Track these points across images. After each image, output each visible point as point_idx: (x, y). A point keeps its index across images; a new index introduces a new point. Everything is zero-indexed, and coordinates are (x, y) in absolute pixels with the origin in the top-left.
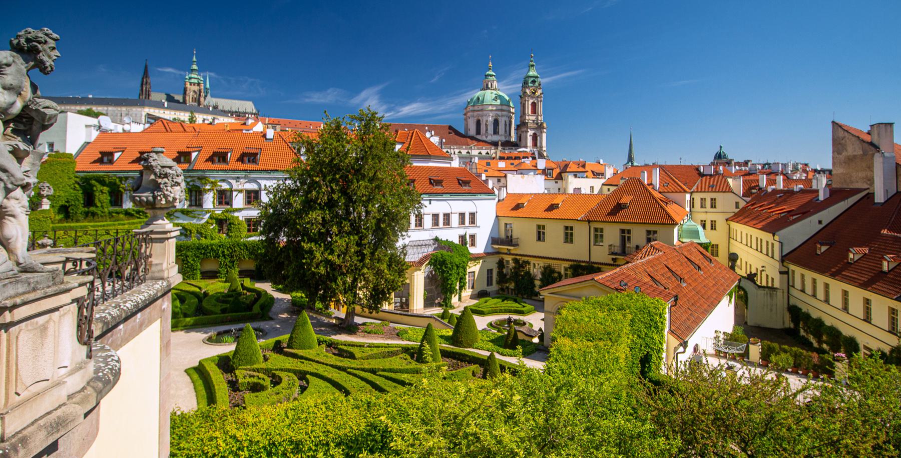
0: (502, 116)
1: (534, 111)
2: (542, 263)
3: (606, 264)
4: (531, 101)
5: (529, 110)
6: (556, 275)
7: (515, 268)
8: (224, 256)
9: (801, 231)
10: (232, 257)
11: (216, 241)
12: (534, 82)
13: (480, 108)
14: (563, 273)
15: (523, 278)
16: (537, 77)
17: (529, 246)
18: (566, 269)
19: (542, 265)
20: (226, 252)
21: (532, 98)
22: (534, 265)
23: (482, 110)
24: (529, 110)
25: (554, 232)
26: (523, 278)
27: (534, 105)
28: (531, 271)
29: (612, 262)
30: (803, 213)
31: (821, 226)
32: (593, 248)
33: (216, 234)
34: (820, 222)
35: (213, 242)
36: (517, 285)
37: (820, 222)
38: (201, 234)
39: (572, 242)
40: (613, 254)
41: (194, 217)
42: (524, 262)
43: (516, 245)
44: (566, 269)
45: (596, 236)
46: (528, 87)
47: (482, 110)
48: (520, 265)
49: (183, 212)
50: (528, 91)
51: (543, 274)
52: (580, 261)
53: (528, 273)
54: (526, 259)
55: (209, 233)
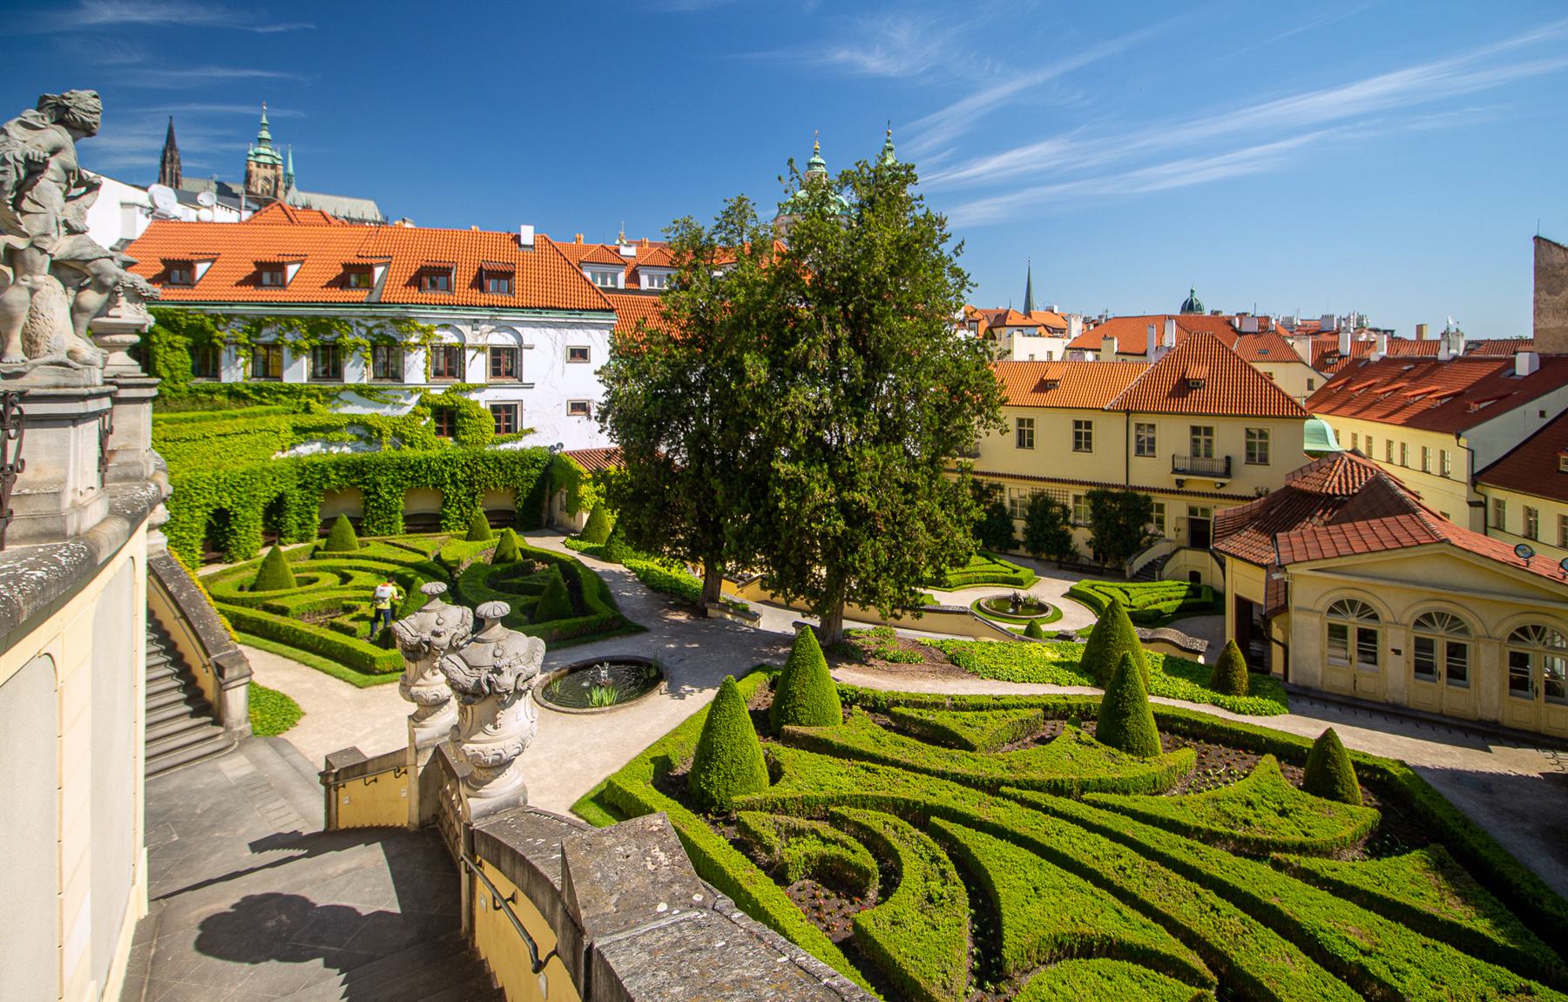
3: (1162, 491)
6: (1056, 510)
8: (454, 482)
9: (1506, 431)
10: (471, 484)
11: (434, 453)
14: (1071, 506)
18: (1077, 499)
20: (460, 476)
30: (1500, 398)
31: (1545, 421)
32: (1134, 459)
33: (431, 438)
34: (1542, 414)
35: (429, 453)
37: (1542, 414)
38: (402, 437)
40: (1175, 471)
41: (385, 402)
42: (991, 486)
43: (976, 455)
44: (1077, 499)
49: (360, 391)
51: (1031, 508)
52: (1109, 485)
55: (418, 435)
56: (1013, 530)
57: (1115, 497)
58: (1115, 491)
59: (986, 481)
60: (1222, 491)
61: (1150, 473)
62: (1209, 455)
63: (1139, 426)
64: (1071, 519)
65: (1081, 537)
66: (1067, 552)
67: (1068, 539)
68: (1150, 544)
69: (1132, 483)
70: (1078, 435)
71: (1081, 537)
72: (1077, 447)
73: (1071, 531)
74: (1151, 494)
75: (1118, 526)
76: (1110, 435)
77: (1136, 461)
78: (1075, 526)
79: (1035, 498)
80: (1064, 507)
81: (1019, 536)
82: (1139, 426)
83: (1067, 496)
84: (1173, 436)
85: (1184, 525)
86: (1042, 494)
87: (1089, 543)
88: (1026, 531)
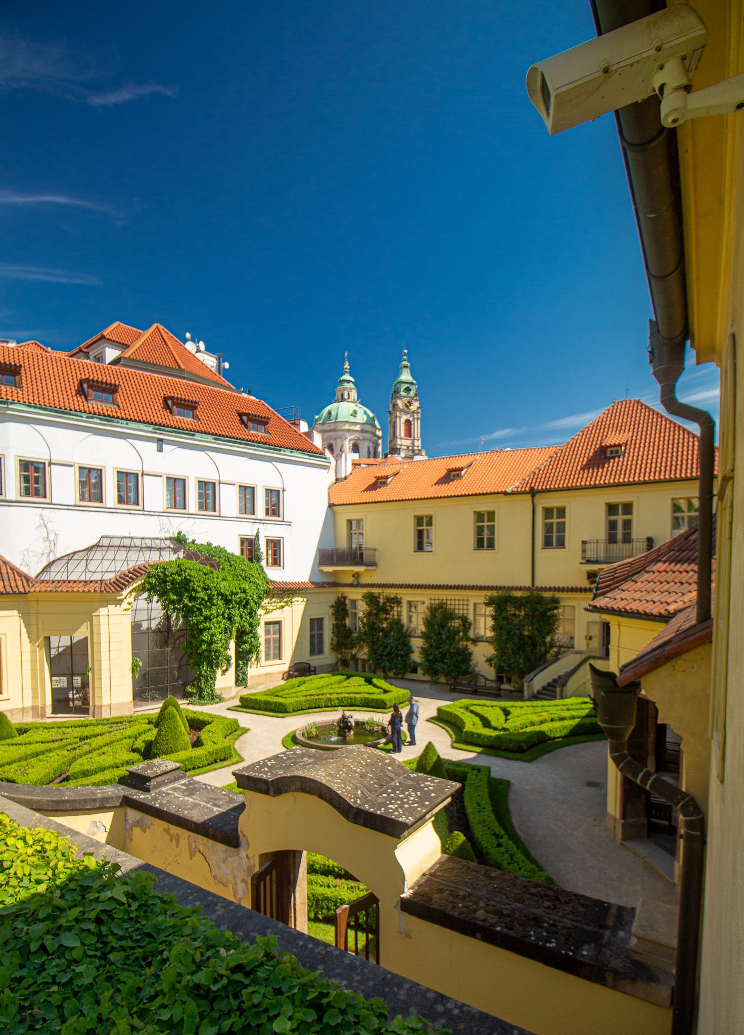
0: (364, 439)
1: (409, 433)
2: (424, 601)
4: (404, 418)
5: (401, 430)
6: (457, 623)
7: (369, 615)
12: (408, 390)
13: (332, 427)
14: (471, 617)
15: (386, 636)
16: (412, 384)
17: (399, 564)
19: (427, 603)
21: (406, 413)
22: (410, 604)
23: (334, 430)
24: (401, 430)
25: (454, 529)
26: (386, 636)
27: (408, 422)
28: (404, 619)
36: (373, 651)
39: (491, 545)
45: (548, 528)
46: (401, 398)
47: (334, 430)
48: (380, 606)
50: (400, 403)
51: (429, 623)
53: (397, 624)
54: (391, 592)
56: (410, 650)
57: (519, 603)
58: (518, 594)
61: (561, 569)
62: (627, 539)
63: (548, 512)
64: (471, 634)
65: (482, 655)
66: (465, 673)
67: (465, 657)
69: (538, 584)
70: (480, 530)
71: (482, 655)
72: (480, 544)
73: (471, 647)
74: (558, 595)
75: (521, 637)
76: (515, 526)
77: (543, 555)
78: (475, 641)
79: (433, 610)
80: (464, 619)
81: (416, 657)
82: (548, 512)
84: (586, 520)
87: (489, 660)
88: (424, 651)
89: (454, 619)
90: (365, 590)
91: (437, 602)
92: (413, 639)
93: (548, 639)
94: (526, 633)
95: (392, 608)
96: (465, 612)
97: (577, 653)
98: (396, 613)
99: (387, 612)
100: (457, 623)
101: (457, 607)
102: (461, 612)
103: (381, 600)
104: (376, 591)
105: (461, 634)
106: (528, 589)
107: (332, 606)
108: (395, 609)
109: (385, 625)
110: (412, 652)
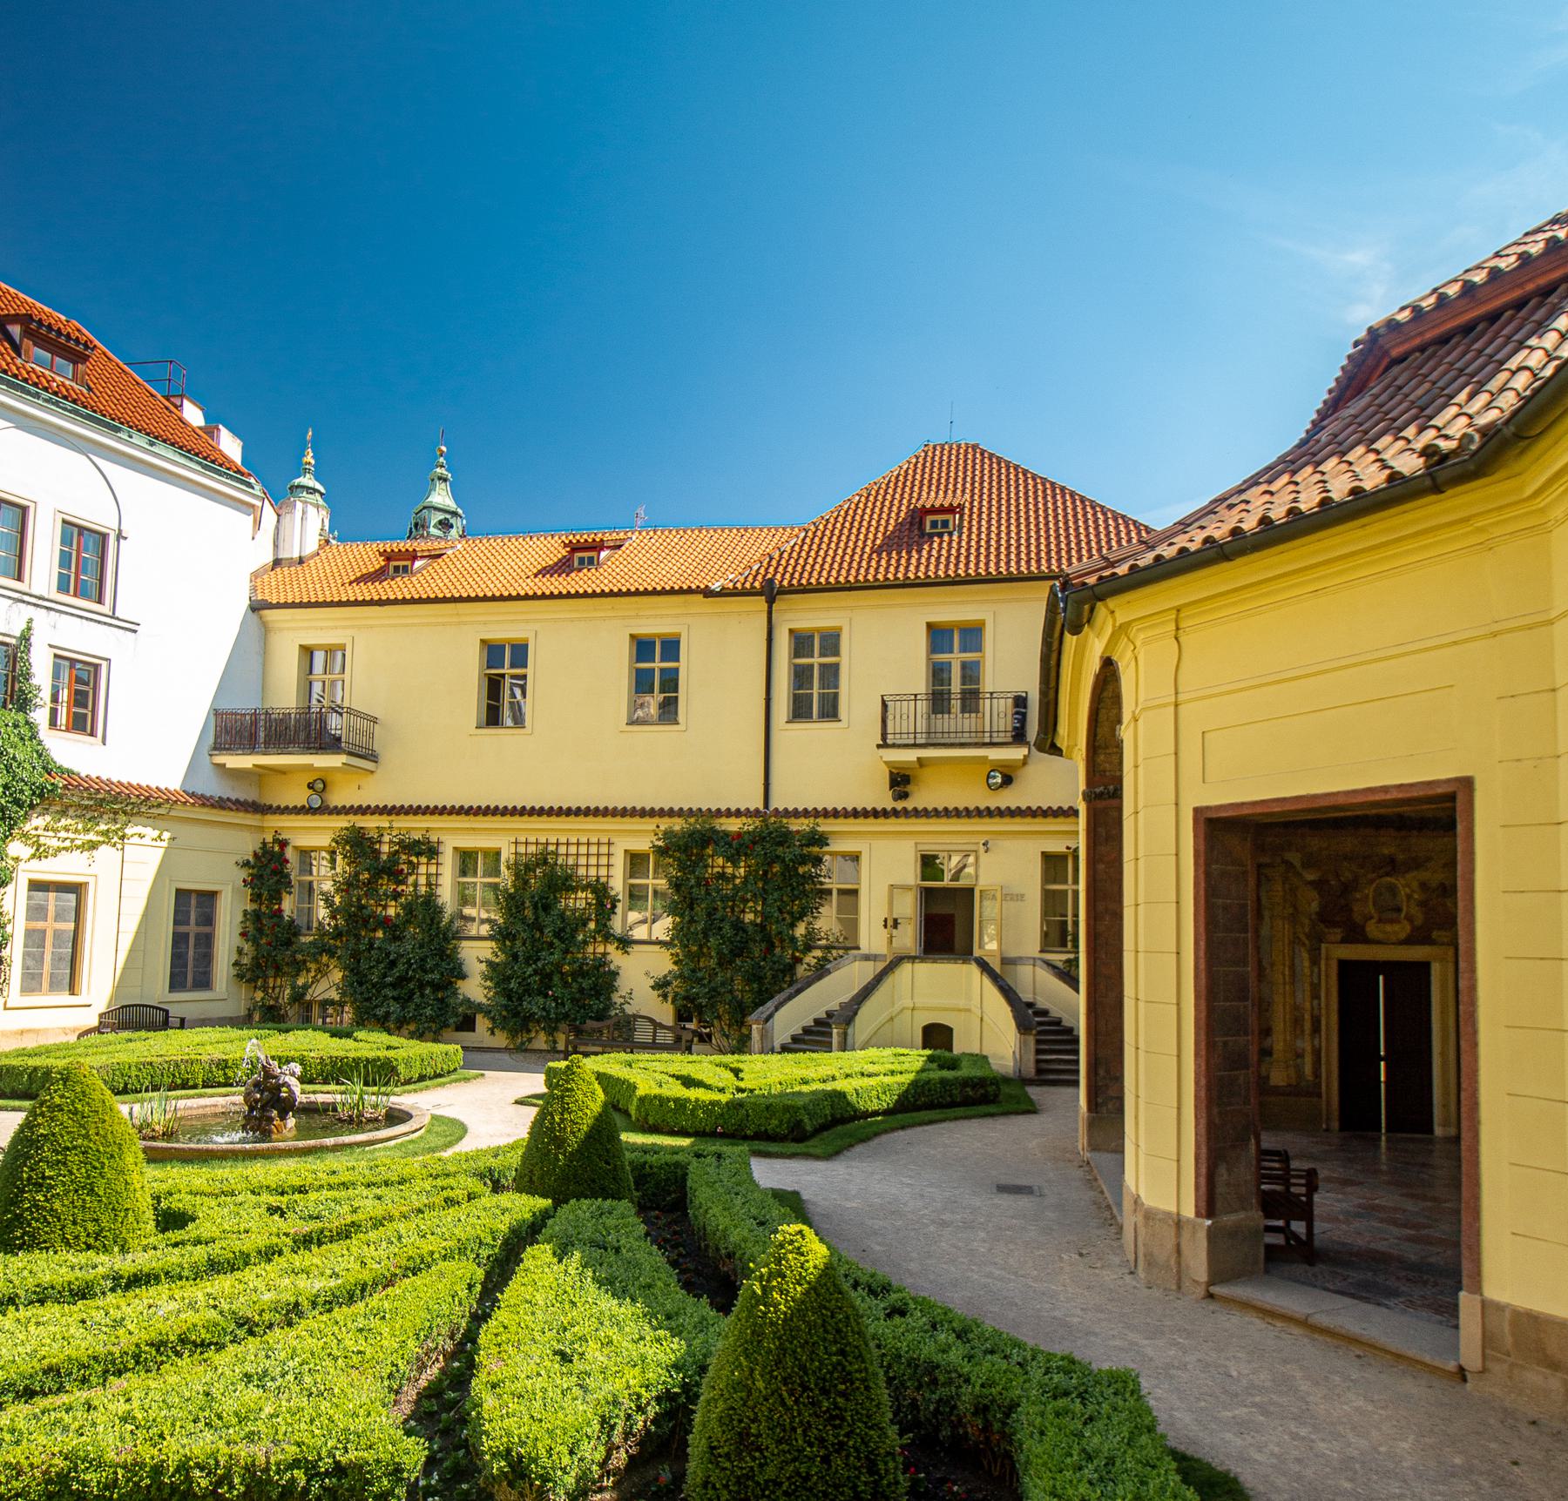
6: (580, 901)
14: (618, 885)
18: (636, 862)
29: (886, 801)
44: (636, 862)
51: (512, 903)
54: (415, 827)
56: (458, 972)
59: (388, 832)
60: (1007, 799)
61: (827, 768)
68: (821, 971)
69: (778, 803)
73: (616, 957)
77: (790, 736)
78: (625, 943)
80: (600, 890)
81: (475, 988)
83: (608, 854)
85: (908, 907)
86: (543, 859)
89: (574, 890)
90: (342, 822)
91: (532, 849)
92: (464, 944)
93: (800, 930)
94: (749, 917)
95: (414, 867)
96: (603, 872)
97: (867, 958)
98: (422, 880)
99: (397, 876)
100: (580, 901)
101: (583, 861)
102: (593, 871)
103: (385, 848)
104: (370, 823)
105: (592, 925)
106: (757, 813)
107: (246, 864)
108: (422, 869)
109: (391, 912)
110: (463, 977)
